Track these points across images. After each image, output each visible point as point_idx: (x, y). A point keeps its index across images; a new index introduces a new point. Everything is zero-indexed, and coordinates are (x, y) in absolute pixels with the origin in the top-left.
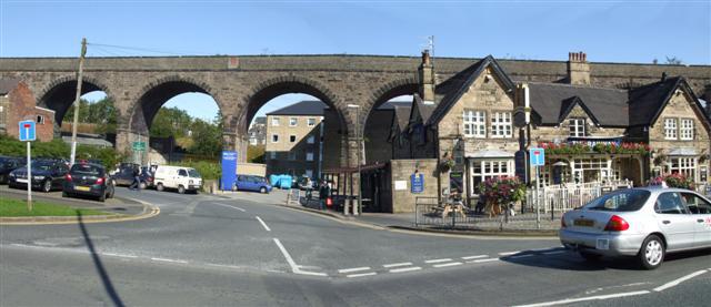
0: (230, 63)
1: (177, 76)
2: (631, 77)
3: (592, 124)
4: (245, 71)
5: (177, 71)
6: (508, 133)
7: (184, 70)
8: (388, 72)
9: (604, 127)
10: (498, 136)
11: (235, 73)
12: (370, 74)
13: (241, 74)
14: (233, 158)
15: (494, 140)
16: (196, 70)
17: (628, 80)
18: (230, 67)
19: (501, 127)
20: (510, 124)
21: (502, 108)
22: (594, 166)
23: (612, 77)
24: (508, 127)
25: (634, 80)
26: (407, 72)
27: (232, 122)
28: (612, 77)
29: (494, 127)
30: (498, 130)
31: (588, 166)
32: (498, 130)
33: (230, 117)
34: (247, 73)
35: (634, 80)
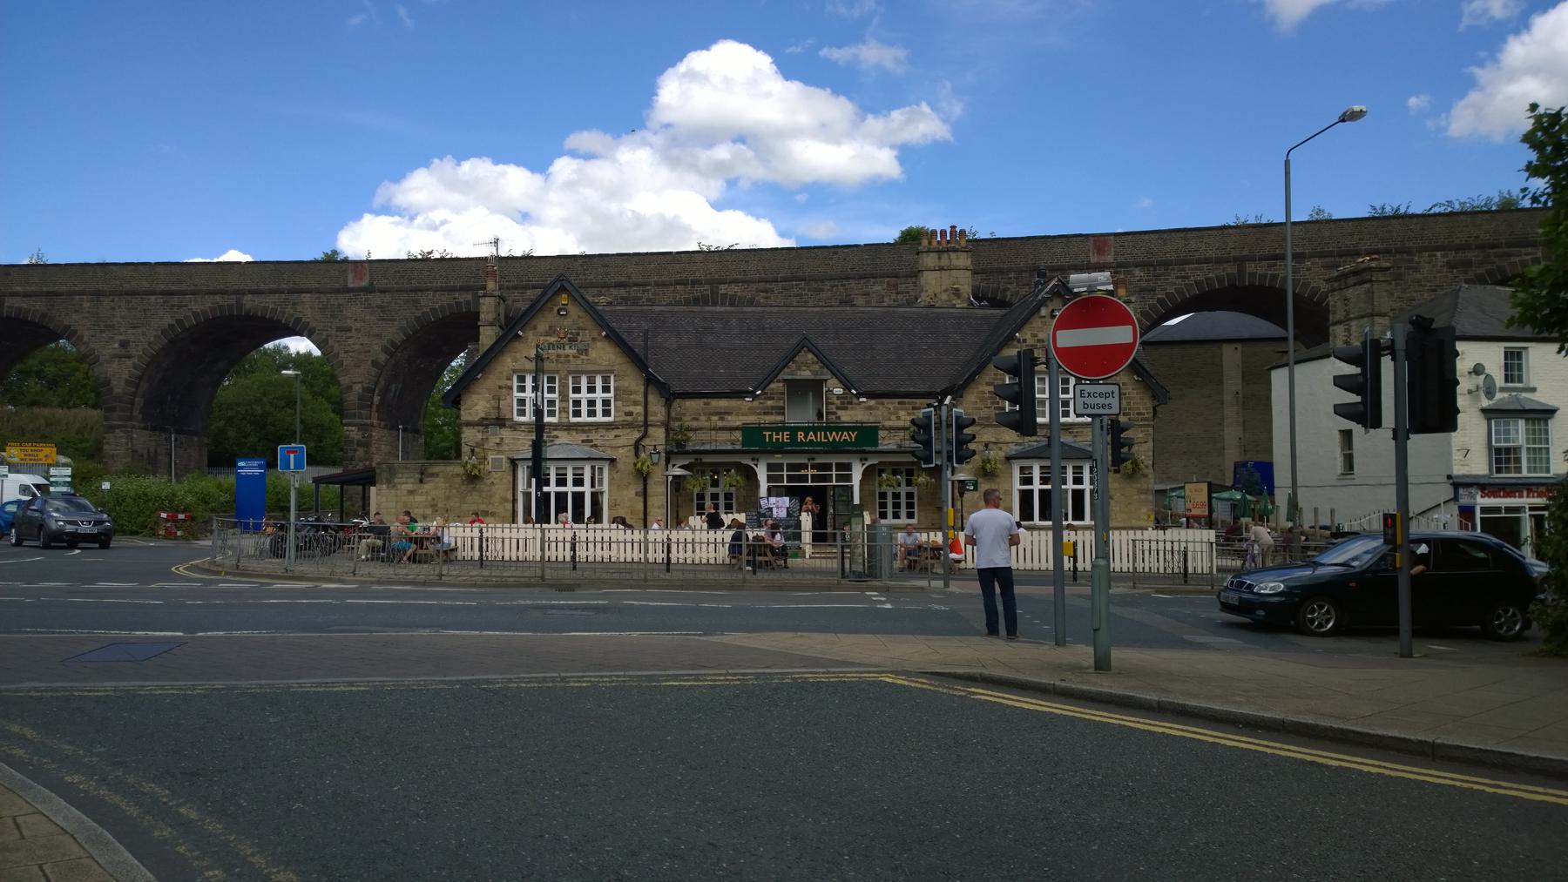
0: (350, 276)
1: (239, 305)
2: (1241, 261)
3: (839, 391)
4: (382, 291)
5: (237, 292)
6: (606, 413)
7: (253, 292)
8: (657, 284)
9: (870, 396)
10: (584, 418)
11: (362, 296)
12: (622, 292)
13: (376, 299)
14: (257, 471)
15: (570, 427)
16: (281, 292)
17: (1232, 269)
18: (351, 285)
19: (592, 403)
20: (611, 395)
21: (590, 367)
22: (815, 478)
23: (1183, 262)
24: (606, 403)
25: (1250, 267)
26: (694, 282)
27: (361, 398)
28: (1183, 262)
29: (577, 403)
30: (584, 408)
31: (804, 478)
32: (584, 408)
33: (358, 388)
34: (388, 297)
35: (1250, 267)
